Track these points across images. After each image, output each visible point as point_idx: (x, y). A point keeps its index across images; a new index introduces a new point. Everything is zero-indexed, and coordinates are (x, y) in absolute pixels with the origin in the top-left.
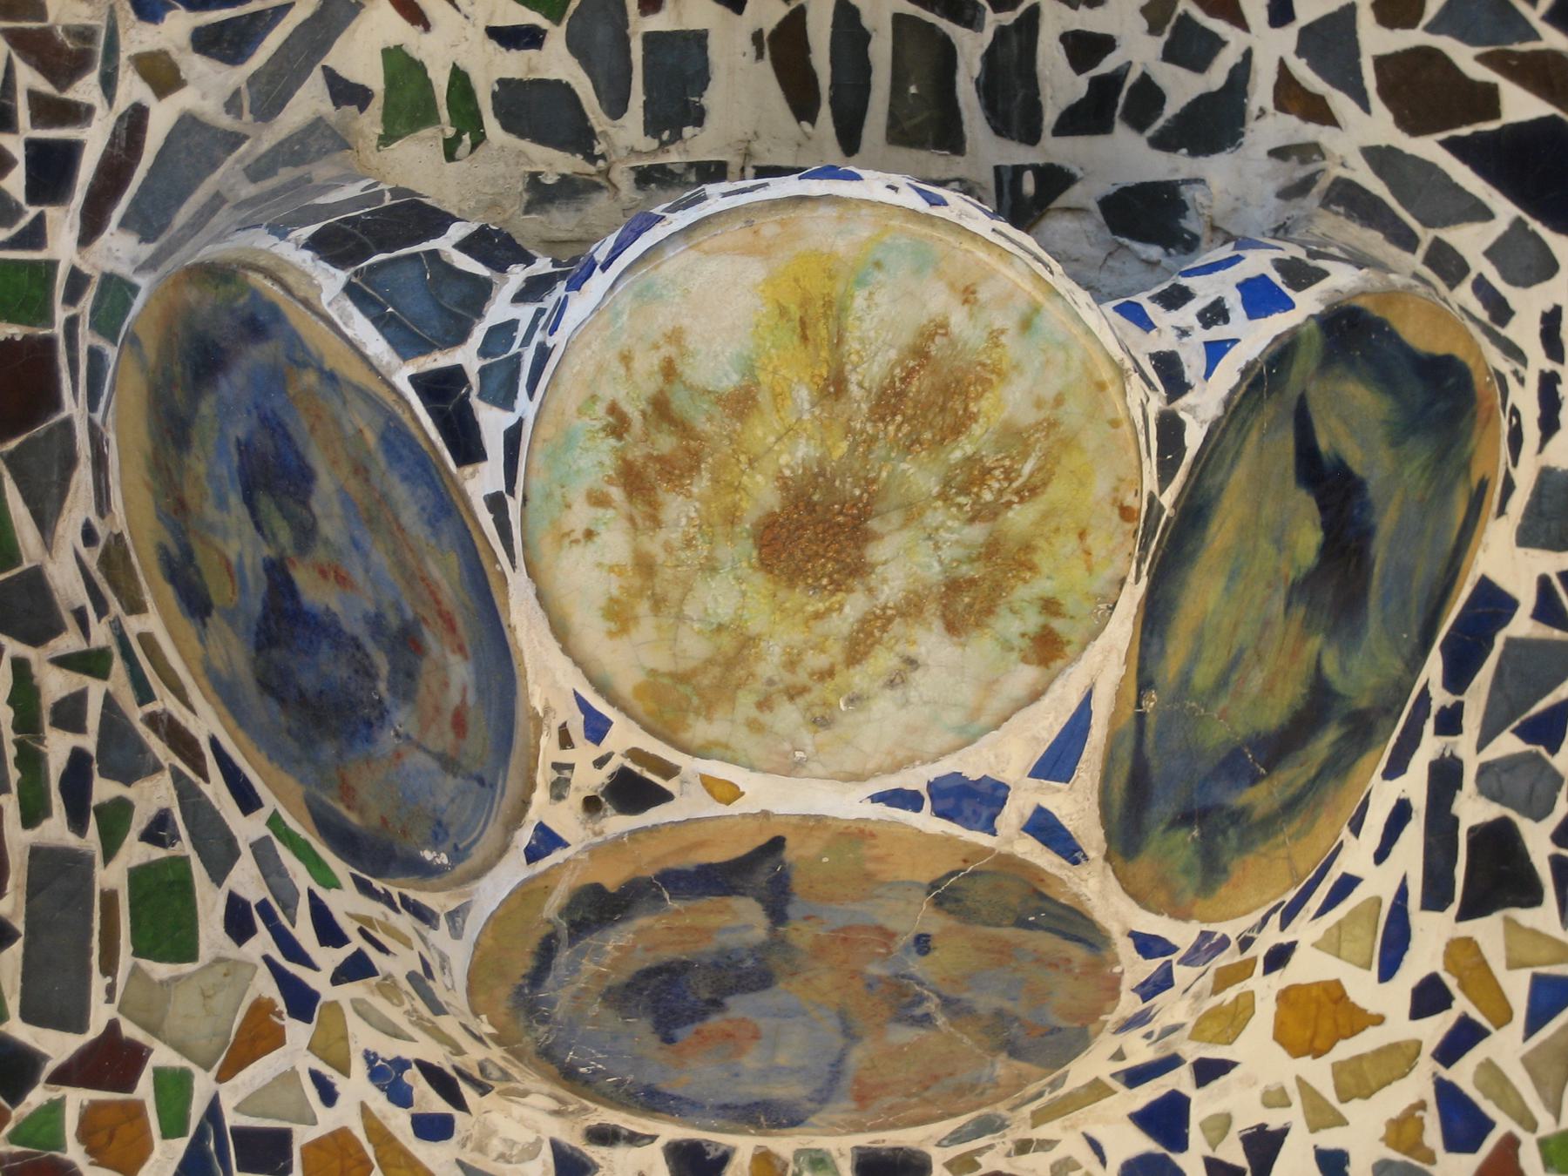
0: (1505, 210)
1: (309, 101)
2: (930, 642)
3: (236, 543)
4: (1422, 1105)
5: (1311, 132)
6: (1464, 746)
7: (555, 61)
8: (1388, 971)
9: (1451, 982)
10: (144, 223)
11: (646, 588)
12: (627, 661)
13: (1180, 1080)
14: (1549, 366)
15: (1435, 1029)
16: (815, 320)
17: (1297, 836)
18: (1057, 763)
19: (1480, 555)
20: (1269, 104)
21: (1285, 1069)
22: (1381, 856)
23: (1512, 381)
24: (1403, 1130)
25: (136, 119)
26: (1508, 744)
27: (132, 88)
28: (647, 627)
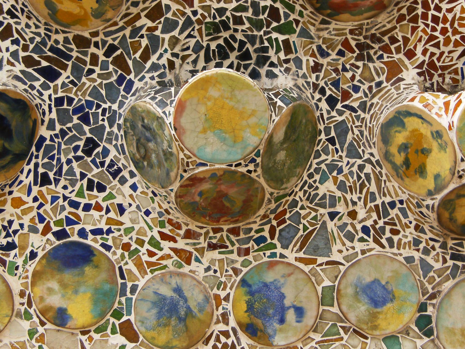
0: (42, 79)
4: (35, 216)
5: (12, 68)
6: (39, 160)
8: (28, 196)
9: (39, 197)
14: (50, 103)
17: (6, 172)
19: (39, 131)
20: (6, 64)
21: (14, 211)
22: (27, 177)
23: (43, 105)
24: (32, 220)
26: (46, 160)
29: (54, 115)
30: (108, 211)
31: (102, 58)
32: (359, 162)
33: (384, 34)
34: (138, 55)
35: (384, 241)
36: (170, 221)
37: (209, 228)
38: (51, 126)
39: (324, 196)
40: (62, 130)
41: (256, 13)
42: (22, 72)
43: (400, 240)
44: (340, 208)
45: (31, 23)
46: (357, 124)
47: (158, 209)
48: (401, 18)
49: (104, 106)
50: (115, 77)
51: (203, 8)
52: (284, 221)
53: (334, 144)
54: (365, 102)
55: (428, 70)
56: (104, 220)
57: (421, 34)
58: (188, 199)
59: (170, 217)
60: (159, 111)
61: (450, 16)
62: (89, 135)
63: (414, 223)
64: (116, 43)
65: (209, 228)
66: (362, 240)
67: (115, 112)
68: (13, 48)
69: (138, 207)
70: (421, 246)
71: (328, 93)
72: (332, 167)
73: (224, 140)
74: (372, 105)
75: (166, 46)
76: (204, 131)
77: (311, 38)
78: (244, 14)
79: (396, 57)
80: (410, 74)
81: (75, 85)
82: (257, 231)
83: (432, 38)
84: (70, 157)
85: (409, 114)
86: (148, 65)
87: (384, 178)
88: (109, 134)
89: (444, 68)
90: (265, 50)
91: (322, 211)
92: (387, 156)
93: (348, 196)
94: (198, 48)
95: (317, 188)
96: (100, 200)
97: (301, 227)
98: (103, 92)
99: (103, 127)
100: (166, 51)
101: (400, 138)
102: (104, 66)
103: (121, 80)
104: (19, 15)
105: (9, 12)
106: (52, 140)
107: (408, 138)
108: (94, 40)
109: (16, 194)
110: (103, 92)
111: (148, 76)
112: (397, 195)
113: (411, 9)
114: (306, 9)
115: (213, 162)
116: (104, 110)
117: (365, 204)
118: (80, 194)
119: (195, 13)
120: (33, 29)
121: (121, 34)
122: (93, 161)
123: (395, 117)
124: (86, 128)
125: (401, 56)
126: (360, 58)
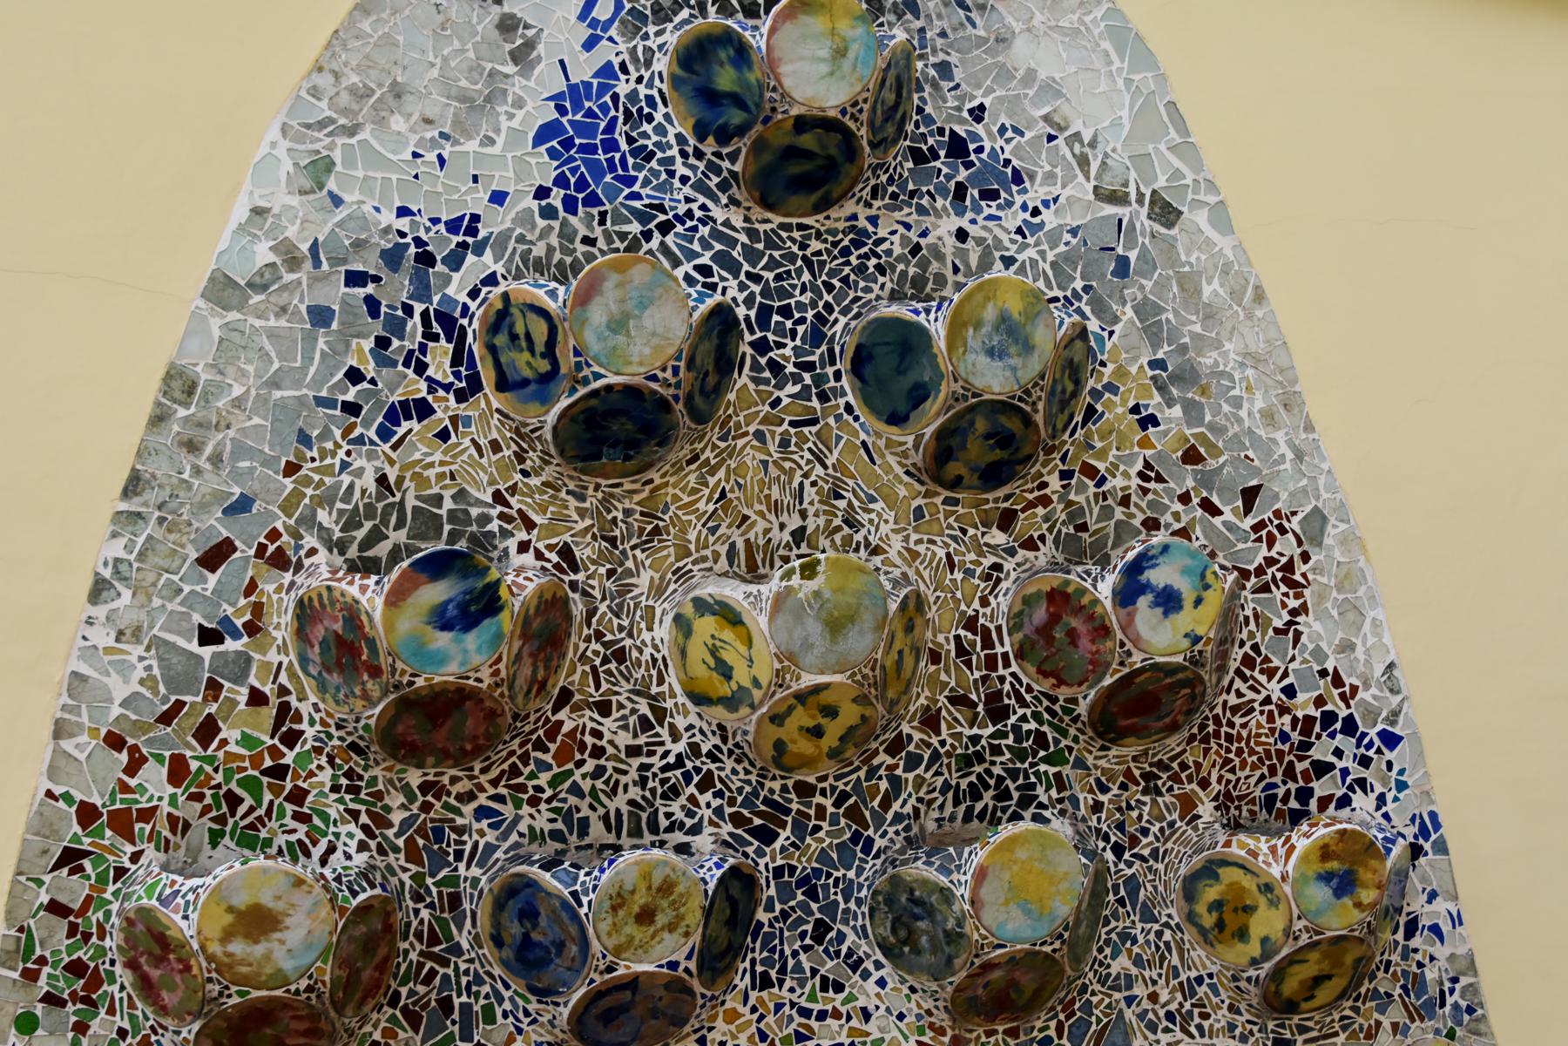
0: (756, 843)
1: (514, 837)
2: (666, 935)
3: (514, 929)
5: (716, 830)
6: (756, 955)
7: (560, 825)
10: (480, 865)
11: (615, 928)
12: (610, 943)
13: (705, 1031)
15: (756, 1016)
16: (647, 876)
18: (689, 957)
25: (476, 844)
26: (765, 954)
27: (475, 837)
28: (614, 936)
29: (772, 891)
30: (849, 1018)
31: (830, 809)
32: (1156, 927)
33: (1172, 759)
34: (876, 803)
35: (1193, 1030)
36: (931, 1026)
37: (981, 1030)
38: (769, 908)
39: (1118, 977)
40: (783, 911)
41: (1018, 740)
42: (730, 834)
43: (1211, 1026)
44: (1139, 990)
45: (739, 768)
46: (1150, 877)
47: (916, 1010)
48: (1192, 738)
49: (836, 874)
50: (848, 835)
51: (952, 735)
52: (1073, 1014)
53: (1124, 906)
54: (1157, 849)
55: (1224, 802)
56: (845, 1032)
57: (1214, 757)
58: (969, 993)
59: (932, 1020)
60: (943, 880)
61: (1244, 733)
62: (818, 916)
63: (1227, 1002)
64: (848, 789)
65: (981, 1030)
66: (1167, 1030)
67: (851, 881)
68: (716, 803)
69: (888, 1010)
70: (1237, 1032)
71: (1113, 839)
72: (1125, 936)
73: (1028, 913)
74: (1165, 852)
75: (910, 788)
76: (1006, 903)
77: (1088, 768)
78: (1003, 742)
79: (1189, 787)
80: (1206, 810)
81: (798, 848)
82: (1041, 1030)
83: (1227, 761)
84: (796, 947)
85: (1225, 863)
86: (890, 816)
87: (1187, 946)
88: (846, 911)
89: (1240, 798)
90: (1033, 786)
91: (1117, 995)
92: (1191, 917)
93: (1147, 974)
94: (946, 787)
95: (1109, 966)
96: (837, 1004)
97: (1094, 1019)
98: (835, 856)
99: (836, 903)
100: (910, 795)
101: (1211, 893)
102: (834, 821)
103: (856, 838)
104: (724, 758)
105: (710, 755)
106: (771, 925)
107: (1222, 893)
108: (820, 785)
109: (728, 1005)
110: (835, 856)
111: (891, 830)
112: (1205, 968)
113: (1203, 727)
114: (1083, 733)
115: (1014, 941)
116: (837, 880)
117: (1168, 983)
118: (812, 998)
119: (943, 743)
120: (742, 776)
121: (854, 776)
122: (826, 951)
123: (1204, 867)
124: (814, 906)
125: (1194, 786)
126: (1145, 792)
